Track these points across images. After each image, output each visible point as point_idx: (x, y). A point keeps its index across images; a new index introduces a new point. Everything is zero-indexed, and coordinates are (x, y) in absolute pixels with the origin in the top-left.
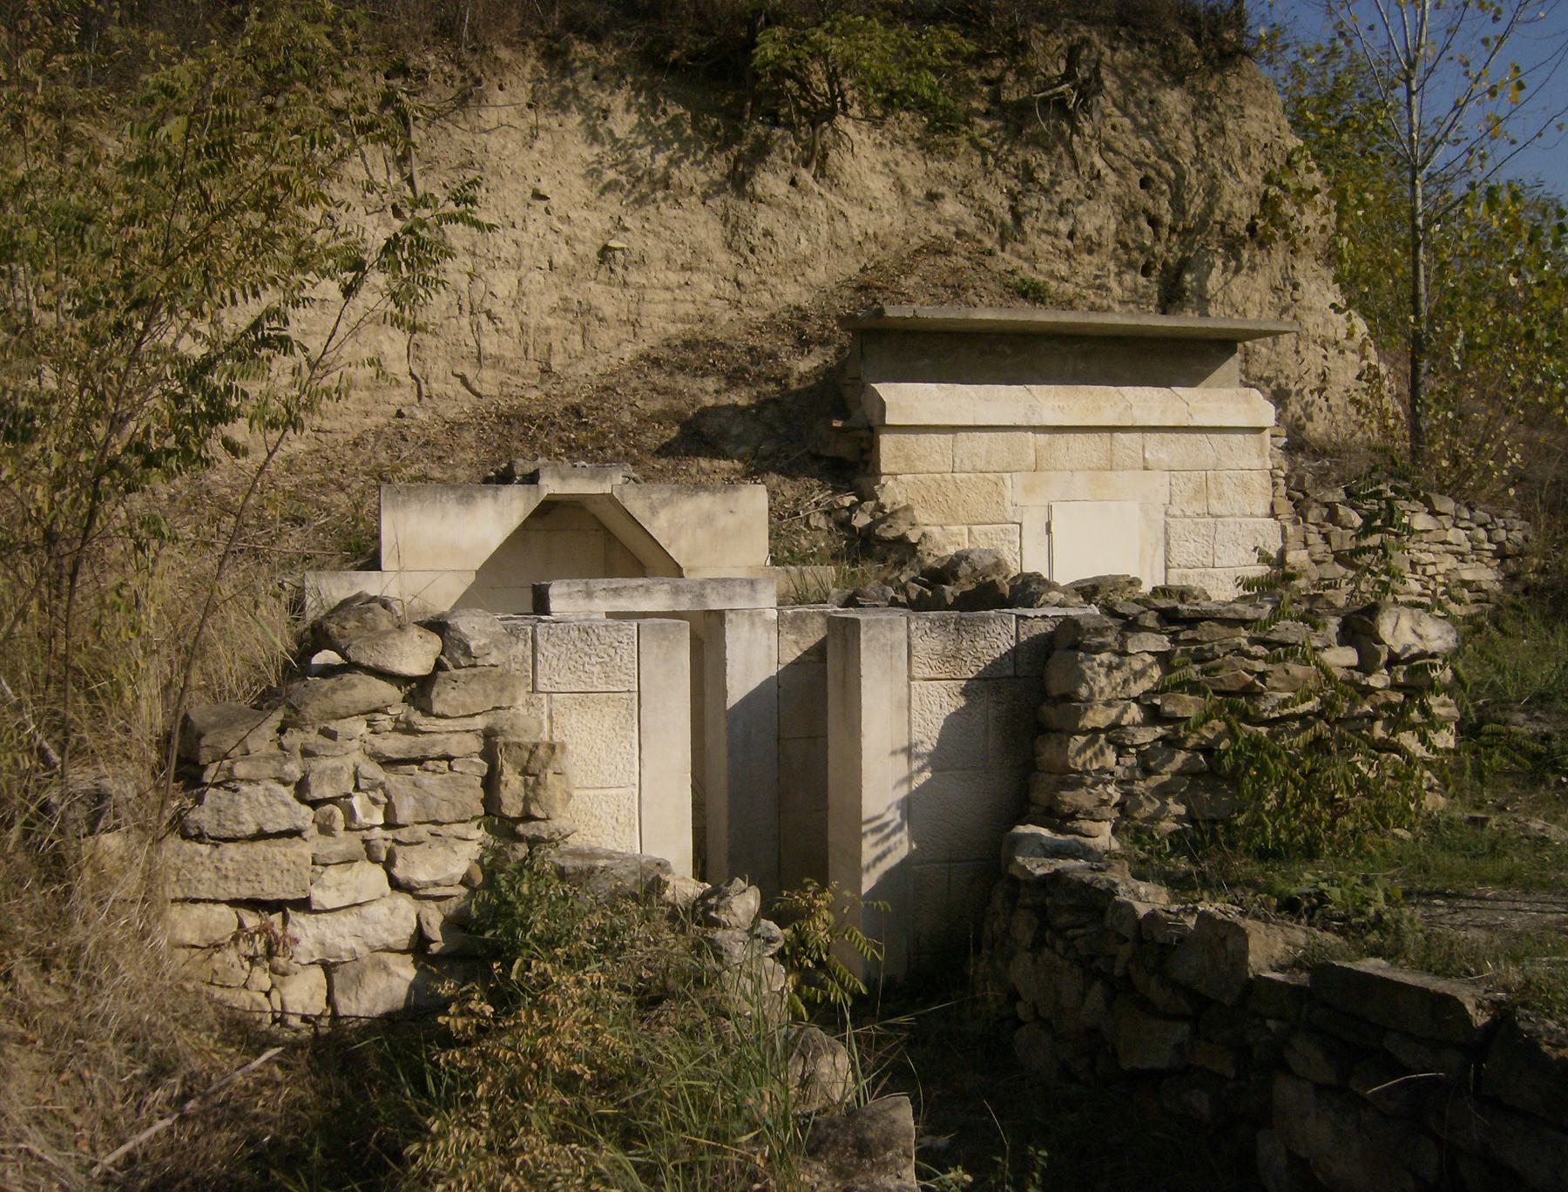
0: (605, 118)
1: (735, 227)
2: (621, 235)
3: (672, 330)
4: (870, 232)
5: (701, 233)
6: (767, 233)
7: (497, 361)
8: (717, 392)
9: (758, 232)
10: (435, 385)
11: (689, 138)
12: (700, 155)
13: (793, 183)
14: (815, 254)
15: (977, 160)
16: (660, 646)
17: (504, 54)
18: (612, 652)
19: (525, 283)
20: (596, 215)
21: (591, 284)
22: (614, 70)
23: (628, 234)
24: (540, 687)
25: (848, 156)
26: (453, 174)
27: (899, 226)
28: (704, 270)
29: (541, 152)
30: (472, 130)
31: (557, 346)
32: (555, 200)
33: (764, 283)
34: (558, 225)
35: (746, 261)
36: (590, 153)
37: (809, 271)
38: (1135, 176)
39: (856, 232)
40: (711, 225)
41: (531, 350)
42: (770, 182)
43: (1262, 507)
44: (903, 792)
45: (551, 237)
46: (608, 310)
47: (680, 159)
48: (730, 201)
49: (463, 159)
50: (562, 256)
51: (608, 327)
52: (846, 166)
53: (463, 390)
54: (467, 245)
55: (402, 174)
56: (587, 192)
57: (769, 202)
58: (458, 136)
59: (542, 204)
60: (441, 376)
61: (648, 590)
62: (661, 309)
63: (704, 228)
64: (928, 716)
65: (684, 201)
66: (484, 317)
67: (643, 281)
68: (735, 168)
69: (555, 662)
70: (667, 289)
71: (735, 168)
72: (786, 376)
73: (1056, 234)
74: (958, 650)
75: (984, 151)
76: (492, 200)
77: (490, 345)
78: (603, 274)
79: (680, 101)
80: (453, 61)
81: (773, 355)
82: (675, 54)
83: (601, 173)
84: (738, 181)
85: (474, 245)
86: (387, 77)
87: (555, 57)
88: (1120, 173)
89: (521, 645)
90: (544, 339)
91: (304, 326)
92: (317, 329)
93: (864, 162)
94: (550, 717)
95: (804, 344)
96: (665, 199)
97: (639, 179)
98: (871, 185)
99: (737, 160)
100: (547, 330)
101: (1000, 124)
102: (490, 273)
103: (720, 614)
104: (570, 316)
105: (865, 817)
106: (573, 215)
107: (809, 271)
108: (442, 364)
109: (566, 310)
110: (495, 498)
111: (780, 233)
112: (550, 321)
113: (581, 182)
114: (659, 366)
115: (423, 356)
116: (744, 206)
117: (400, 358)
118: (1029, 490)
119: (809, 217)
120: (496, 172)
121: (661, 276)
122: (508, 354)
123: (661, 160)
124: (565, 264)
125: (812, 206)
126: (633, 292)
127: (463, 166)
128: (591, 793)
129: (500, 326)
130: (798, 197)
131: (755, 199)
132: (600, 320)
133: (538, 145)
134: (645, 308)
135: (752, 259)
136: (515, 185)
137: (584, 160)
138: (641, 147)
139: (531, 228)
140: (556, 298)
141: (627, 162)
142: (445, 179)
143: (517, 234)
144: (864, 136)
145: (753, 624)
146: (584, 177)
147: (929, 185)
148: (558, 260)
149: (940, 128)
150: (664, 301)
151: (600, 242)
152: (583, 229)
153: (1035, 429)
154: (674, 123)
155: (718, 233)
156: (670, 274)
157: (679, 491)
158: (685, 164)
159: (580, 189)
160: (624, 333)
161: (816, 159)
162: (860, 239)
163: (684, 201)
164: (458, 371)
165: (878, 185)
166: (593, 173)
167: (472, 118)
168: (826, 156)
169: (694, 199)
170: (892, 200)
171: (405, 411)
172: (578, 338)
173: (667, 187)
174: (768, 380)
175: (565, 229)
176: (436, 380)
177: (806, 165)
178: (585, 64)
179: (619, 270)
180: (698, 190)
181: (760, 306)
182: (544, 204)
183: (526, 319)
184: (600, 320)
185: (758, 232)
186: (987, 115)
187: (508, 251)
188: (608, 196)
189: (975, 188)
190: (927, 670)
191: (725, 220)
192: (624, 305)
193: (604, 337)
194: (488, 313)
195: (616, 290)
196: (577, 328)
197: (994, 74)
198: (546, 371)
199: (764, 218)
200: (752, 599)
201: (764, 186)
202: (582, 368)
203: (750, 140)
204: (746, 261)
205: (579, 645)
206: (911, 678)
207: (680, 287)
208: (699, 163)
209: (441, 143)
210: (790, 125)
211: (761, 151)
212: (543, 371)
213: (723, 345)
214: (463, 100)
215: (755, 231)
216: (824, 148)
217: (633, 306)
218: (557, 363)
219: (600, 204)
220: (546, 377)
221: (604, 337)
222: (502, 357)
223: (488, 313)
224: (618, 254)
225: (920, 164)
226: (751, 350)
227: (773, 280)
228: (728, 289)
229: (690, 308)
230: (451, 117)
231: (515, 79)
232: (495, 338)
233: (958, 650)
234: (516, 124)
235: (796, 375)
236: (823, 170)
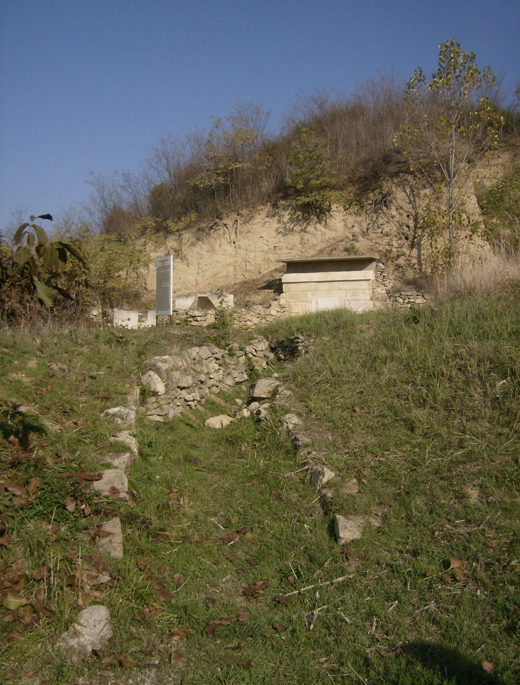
5: (295, 241)
7: (249, 271)
9: (306, 240)
14: (318, 243)
17: (261, 207)
36: (277, 226)
38: (405, 214)
42: (310, 229)
43: (368, 298)
57: (309, 233)
73: (377, 233)
87: (275, 205)
88: (401, 214)
106: (270, 240)
111: (310, 240)
118: (313, 295)
148: (264, 250)
153: (315, 282)
154: (298, 217)
159: (274, 234)
175: (267, 243)
177: (320, 223)
178: (282, 205)
185: (306, 240)
187: (253, 248)
188: (280, 235)
199: (307, 237)
209: (244, 228)
228: (299, 253)
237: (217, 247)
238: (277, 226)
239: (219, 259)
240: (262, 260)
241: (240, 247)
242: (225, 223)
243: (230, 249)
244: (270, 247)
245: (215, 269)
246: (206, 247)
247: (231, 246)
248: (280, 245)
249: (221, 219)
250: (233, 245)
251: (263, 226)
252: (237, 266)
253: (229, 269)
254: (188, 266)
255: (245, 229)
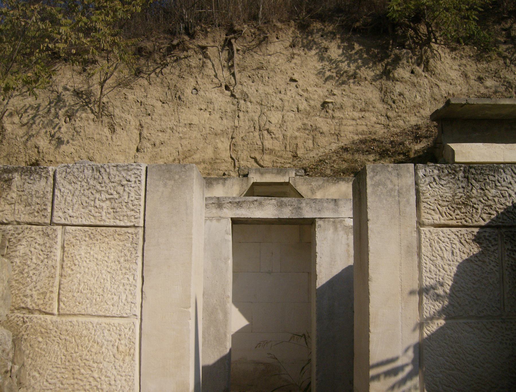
0: (326, 51)
1: (386, 92)
2: (332, 97)
3: (356, 138)
4: (451, 92)
5: (370, 95)
6: (400, 94)
7: (271, 151)
8: (374, 160)
10: (242, 162)
11: (365, 58)
12: (371, 65)
13: (412, 72)
15: (501, 62)
16: (165, 185)
17: (279, 25)
18: (120, 189)
19: (285, 117)
20: (320, 89)
21: (317, 118)
22: (332, 33)
23: (335, 97)
24: (56, 220)
25: (439, 62)
26: (253, 72)
27: (465, 91)
28: (371, 111)
29: (295, 64)
30: (264, 55)
31: (300, 145)
32: (300, 82)
33: (400, 116)
34: (301, 93)
35: (391, 107)
36: (319, 66)
37: (421, 111)
39: (444, 92)
40: (374, 92)
41: (288, 147)
42: (402, 72)
44: (415, 338)
45: (298, 97)
46: (325, 128)
47: (361, 67)
48: (383, 82)
49: (259, 66)
50: (304, 105)
51: (325, 137)
52: (438, 66)
53: (255, 164)
54: (259, 101)
55: (230, 72)
56: (317, 80)
57: (401, 80)
58: (256, 57)
59: (294, 84)
60: (245, 158)
61: (260, 204)
62: (351, 128)
63: (371, 93)
64: (439, 262)
65: (362, 84)
66: (266, 132)
67: (342, 116)
68: (386, 68)
69: (69, 199)
70: (353, 119)
71: (386, 68)
72: (408, 152)
74: (469, 197)
75: (505, 58)
76: (270, 82)
77: (268, 144)
78: (323, 114)
79: (360, 44)
80: (255, 27)
81: (402, 143)
82: (358, 24)
83: (325, 73)
84: (386, 74)
85: (262, 101)
86: (226, 35)
87: (303, 27)
89: (43, 183)
90: (294, 141)
91: (181, 135)
92: (187, 136)
93: (447, 65)
94: (63, 247)
95: (417, 138)
96: (354, 83)
97: (342, 75)
98: (451, 74)
99: (387, 65)
100: (296, 138)
101: (511, 46)
102: (269, 112)
103: (312, 222)
104: (307, 132)
105: (373, 361)
106: (309, 89)
107: (421, 111)
108: (245, 153)
109: (305, 129)
110: (224, 184)
111: (407, 94)
112: (297, 134)
113: (314, 76)
114: (348, 151)
115: (237, 149)
116: (390, 83)
117: (226, 150)
119: (420, 86)
120: (273, 70)
121: (351, 114)
122: (277, 148)
123: (353, 67)
124: (305, 109)
125: (421, 82)
126: (337, 121)
127: (258, 68)
128: (95, 320)
129: (273, 136)
130: (415, 78)
131: (394, 80)
132: (321, 133)
133: (294, 61)
134: (342, 128)
135: (394, 106)
136: (282, 76)
137: (316, 68)
138: (343, 62)
139: (289, 93)
140: (300, 124)
141: (335, 68)
142: (249, 74)
143: (282, 96)
144: (447, 55)
145: (336, 229)
146: (316, 75)
147: (479, 74)
148: (301, 107)
149: (483, 51)
150: (352, 125)
151: (322, 100)
152: (314, 94)
155: (378, 96)
156: (355, 113)
157: (328, 181)
158: (363, 69)
159: (313, 78)
160: (333, 139)
161: (424, 63)
162: (446, 95)
163: (362, 84)
164: (253, 156)
165: (454, 74)
166: (320, 73)
167: (263, 49)
168: (428, 62)
169: (367, 82)
170: (461, 80)
171: (226, 173)
172: (311, 141)
173: (355, 78)
174: (399, 154)
175: (305, 94)
176: (243, 160)
177: (419, 65)
179: (330, 112)
180: (369, 78)
181: (398, 127)
182: (295, 84)
183: (285, 133)
184: (321, 133)
186: (505, 43)
188: (328, 82)
189: (501, 74)
190: (437, 216)
191: (381, 90)
192: (333, 127)
193: (323, 141)
194: (268, 130)
195: (329, 120)
196: (310, 137)
197: (507, 26)
198: (295, 156)
199: (399, 87)
200: (336, 211)
201: (398, 74)
202: (312, 154)
203: (393, 56)
204: (391, 107)
205: (92, 182)
206: (420, 224)
207: (359, 118)
208: (370, 68)
209: (248, 60)
210: (410, 48)
211: (397, 60)
212: (294, 156)
213: (379, 141)
214: (259, 44)
215: (395, 93)
216: (427, 59)
217: (337, 127)
218: (300, 153)
219: (324, 85)
220: (295, 159)
221: (323, 141)
222: (274, 149)
223: (268, 130)
224: (330, 105)
225: (474, 67)
226: (391, 142)
227: (405, 115)
228: (383, 119)
229: (365, 128)
230: (254, 50)
231: (284, 35)
232: (271, 141)
233: (469, 197)
234: (284, 52)
235: (413, 151)
236: (427, 68)
237: (188, 91)
238: (319, 66)
239: (195, 120)
240: (299, 129)
241: (245, 97)
242: (200, 44)
243: (221, 99)
244: (312, 103)
245: (185, 142)
246: (156, 92)
247: (222, 93)
248: (338, 100)
249: (192, 36)
250: (227, 92)
251: (289, 61)
252: (238, 139)
253: (220, 145)
254: (113, 130)
255: (253, 60)
